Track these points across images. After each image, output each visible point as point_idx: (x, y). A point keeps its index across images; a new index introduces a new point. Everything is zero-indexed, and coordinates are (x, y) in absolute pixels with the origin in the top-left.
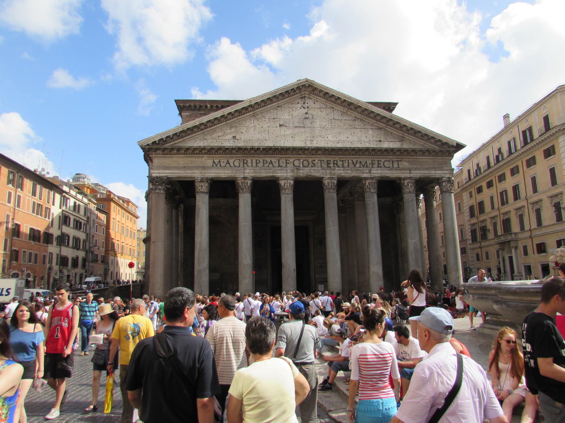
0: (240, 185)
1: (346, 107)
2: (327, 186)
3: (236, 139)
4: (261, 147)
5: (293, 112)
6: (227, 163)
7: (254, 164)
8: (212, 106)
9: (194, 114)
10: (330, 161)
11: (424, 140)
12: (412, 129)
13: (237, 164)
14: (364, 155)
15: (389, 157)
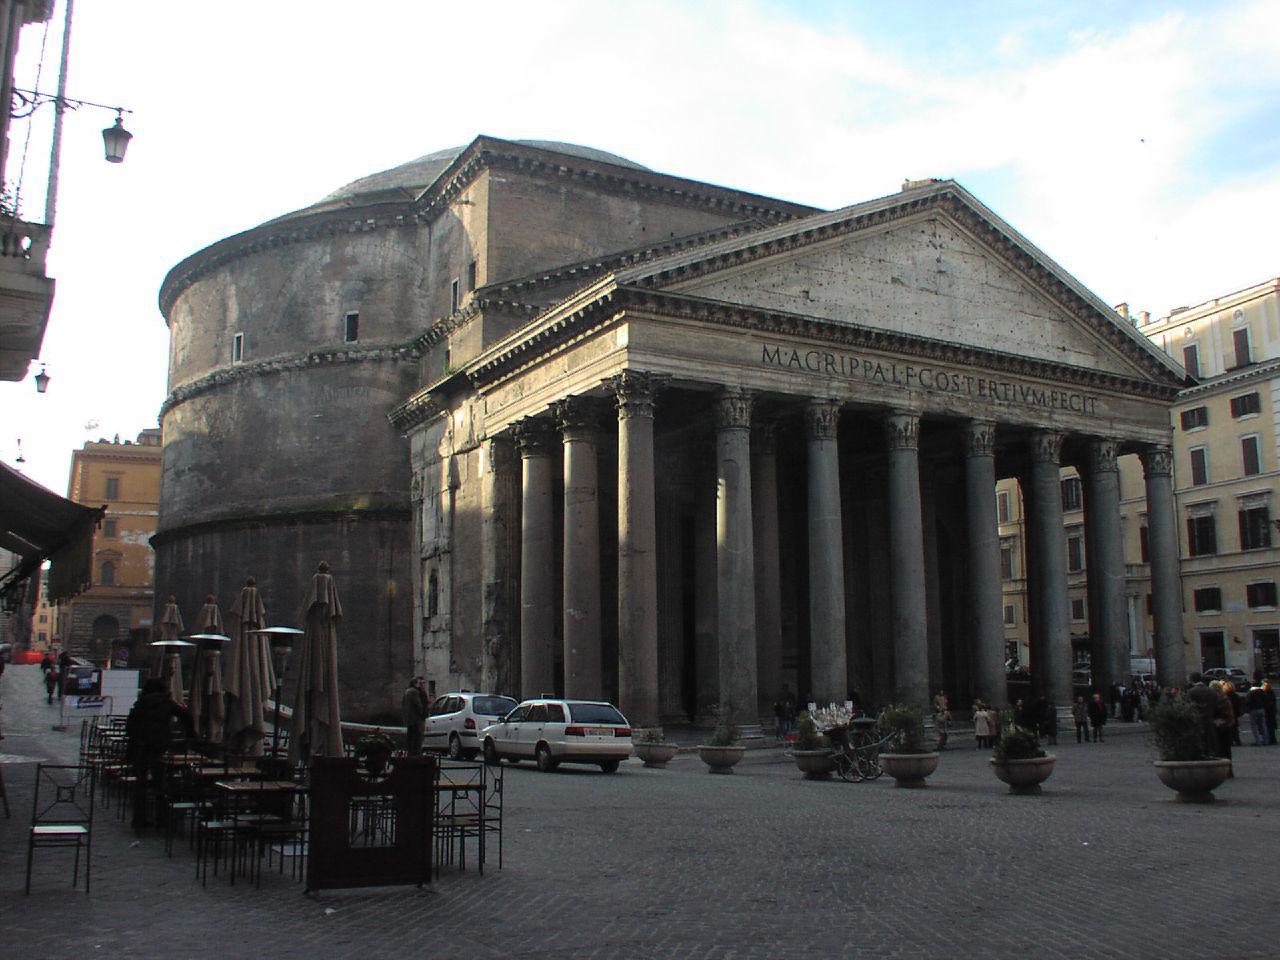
0: (819, 418)
1: (1011, 262)
2: (978, 438)
3: (808, 298)
4: (876, 331)
5: (916, 253)
6: (792, 359)
7: (847, 369)
8: (570, 171)
9: (520, 184)
10: (984, 381)
11: (1132, 360)
12: (1120, 332)
13: (813, 363)
14: (1043, 377)
15: (1080, 387)
